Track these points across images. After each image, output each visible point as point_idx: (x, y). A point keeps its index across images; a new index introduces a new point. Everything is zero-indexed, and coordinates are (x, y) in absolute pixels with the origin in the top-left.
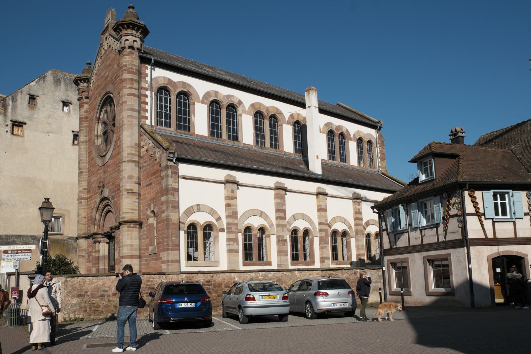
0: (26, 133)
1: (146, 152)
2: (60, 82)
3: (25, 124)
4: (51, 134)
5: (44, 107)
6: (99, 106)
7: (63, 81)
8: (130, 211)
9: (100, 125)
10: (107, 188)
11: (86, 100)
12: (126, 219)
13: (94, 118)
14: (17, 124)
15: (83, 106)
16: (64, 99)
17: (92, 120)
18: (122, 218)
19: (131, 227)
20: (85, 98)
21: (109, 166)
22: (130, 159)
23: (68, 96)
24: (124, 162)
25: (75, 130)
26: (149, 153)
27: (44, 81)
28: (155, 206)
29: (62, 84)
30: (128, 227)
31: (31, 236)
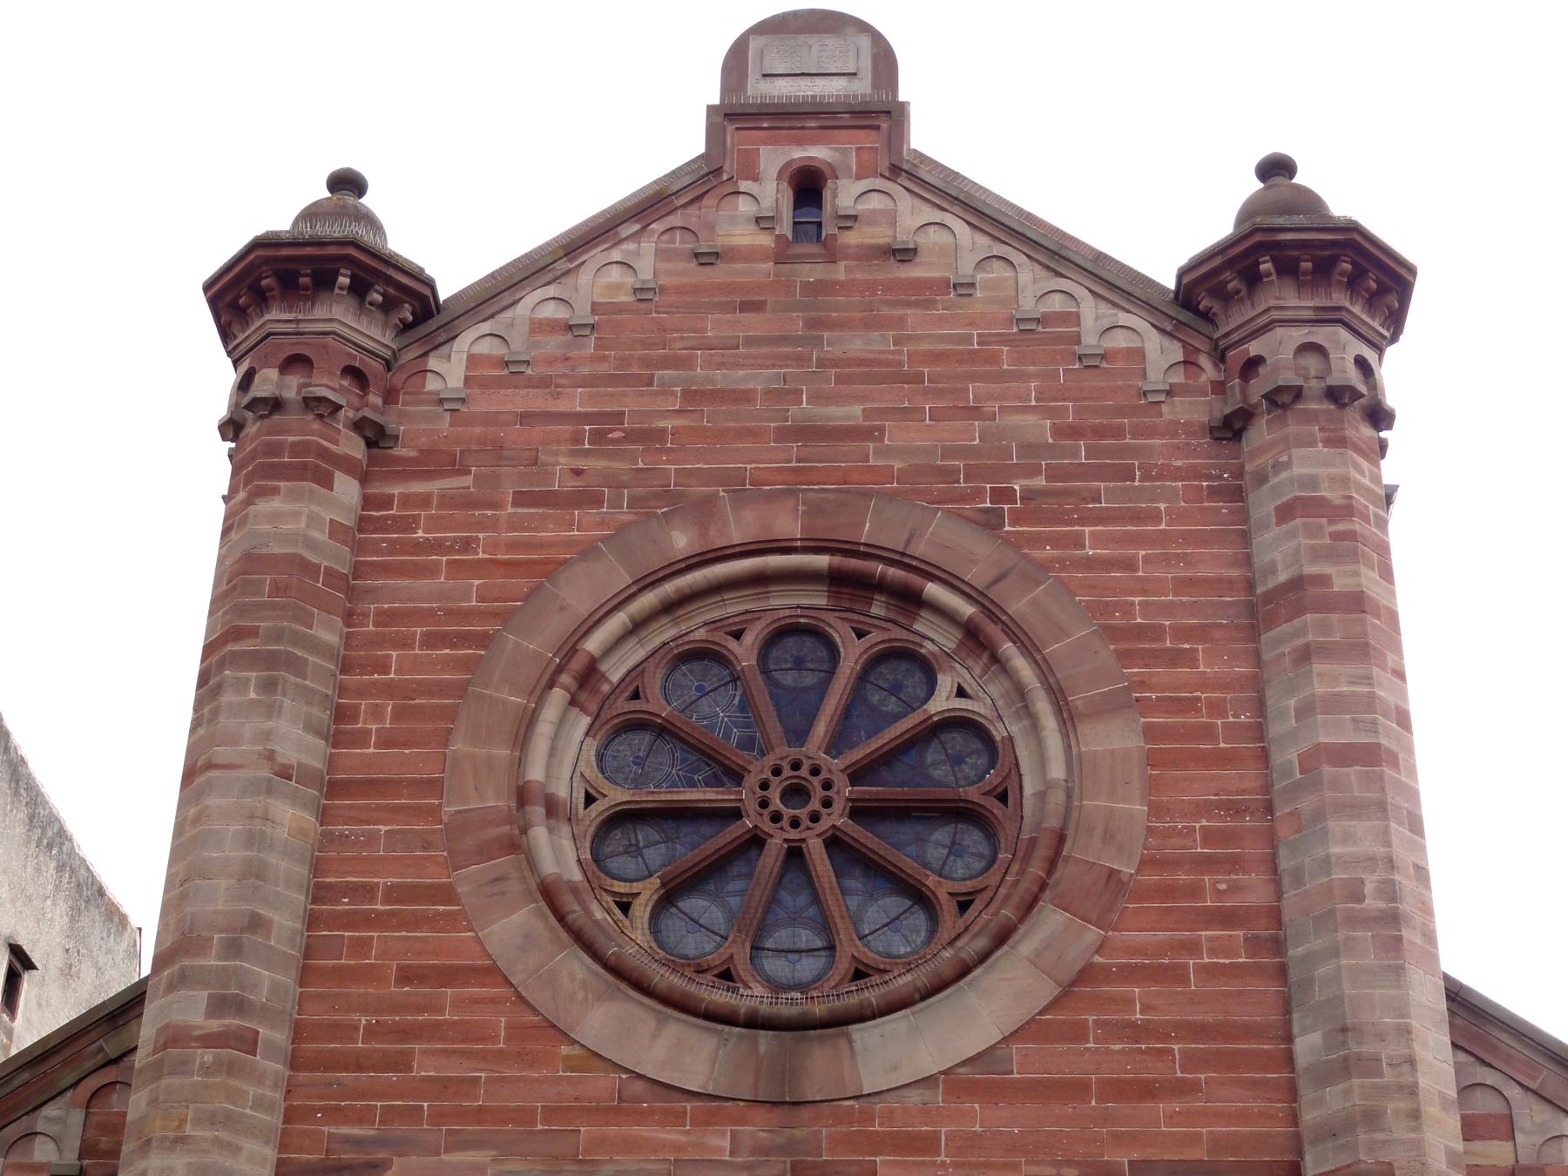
11: (353, 447)
13: (536, 642)
20: (359, 426)
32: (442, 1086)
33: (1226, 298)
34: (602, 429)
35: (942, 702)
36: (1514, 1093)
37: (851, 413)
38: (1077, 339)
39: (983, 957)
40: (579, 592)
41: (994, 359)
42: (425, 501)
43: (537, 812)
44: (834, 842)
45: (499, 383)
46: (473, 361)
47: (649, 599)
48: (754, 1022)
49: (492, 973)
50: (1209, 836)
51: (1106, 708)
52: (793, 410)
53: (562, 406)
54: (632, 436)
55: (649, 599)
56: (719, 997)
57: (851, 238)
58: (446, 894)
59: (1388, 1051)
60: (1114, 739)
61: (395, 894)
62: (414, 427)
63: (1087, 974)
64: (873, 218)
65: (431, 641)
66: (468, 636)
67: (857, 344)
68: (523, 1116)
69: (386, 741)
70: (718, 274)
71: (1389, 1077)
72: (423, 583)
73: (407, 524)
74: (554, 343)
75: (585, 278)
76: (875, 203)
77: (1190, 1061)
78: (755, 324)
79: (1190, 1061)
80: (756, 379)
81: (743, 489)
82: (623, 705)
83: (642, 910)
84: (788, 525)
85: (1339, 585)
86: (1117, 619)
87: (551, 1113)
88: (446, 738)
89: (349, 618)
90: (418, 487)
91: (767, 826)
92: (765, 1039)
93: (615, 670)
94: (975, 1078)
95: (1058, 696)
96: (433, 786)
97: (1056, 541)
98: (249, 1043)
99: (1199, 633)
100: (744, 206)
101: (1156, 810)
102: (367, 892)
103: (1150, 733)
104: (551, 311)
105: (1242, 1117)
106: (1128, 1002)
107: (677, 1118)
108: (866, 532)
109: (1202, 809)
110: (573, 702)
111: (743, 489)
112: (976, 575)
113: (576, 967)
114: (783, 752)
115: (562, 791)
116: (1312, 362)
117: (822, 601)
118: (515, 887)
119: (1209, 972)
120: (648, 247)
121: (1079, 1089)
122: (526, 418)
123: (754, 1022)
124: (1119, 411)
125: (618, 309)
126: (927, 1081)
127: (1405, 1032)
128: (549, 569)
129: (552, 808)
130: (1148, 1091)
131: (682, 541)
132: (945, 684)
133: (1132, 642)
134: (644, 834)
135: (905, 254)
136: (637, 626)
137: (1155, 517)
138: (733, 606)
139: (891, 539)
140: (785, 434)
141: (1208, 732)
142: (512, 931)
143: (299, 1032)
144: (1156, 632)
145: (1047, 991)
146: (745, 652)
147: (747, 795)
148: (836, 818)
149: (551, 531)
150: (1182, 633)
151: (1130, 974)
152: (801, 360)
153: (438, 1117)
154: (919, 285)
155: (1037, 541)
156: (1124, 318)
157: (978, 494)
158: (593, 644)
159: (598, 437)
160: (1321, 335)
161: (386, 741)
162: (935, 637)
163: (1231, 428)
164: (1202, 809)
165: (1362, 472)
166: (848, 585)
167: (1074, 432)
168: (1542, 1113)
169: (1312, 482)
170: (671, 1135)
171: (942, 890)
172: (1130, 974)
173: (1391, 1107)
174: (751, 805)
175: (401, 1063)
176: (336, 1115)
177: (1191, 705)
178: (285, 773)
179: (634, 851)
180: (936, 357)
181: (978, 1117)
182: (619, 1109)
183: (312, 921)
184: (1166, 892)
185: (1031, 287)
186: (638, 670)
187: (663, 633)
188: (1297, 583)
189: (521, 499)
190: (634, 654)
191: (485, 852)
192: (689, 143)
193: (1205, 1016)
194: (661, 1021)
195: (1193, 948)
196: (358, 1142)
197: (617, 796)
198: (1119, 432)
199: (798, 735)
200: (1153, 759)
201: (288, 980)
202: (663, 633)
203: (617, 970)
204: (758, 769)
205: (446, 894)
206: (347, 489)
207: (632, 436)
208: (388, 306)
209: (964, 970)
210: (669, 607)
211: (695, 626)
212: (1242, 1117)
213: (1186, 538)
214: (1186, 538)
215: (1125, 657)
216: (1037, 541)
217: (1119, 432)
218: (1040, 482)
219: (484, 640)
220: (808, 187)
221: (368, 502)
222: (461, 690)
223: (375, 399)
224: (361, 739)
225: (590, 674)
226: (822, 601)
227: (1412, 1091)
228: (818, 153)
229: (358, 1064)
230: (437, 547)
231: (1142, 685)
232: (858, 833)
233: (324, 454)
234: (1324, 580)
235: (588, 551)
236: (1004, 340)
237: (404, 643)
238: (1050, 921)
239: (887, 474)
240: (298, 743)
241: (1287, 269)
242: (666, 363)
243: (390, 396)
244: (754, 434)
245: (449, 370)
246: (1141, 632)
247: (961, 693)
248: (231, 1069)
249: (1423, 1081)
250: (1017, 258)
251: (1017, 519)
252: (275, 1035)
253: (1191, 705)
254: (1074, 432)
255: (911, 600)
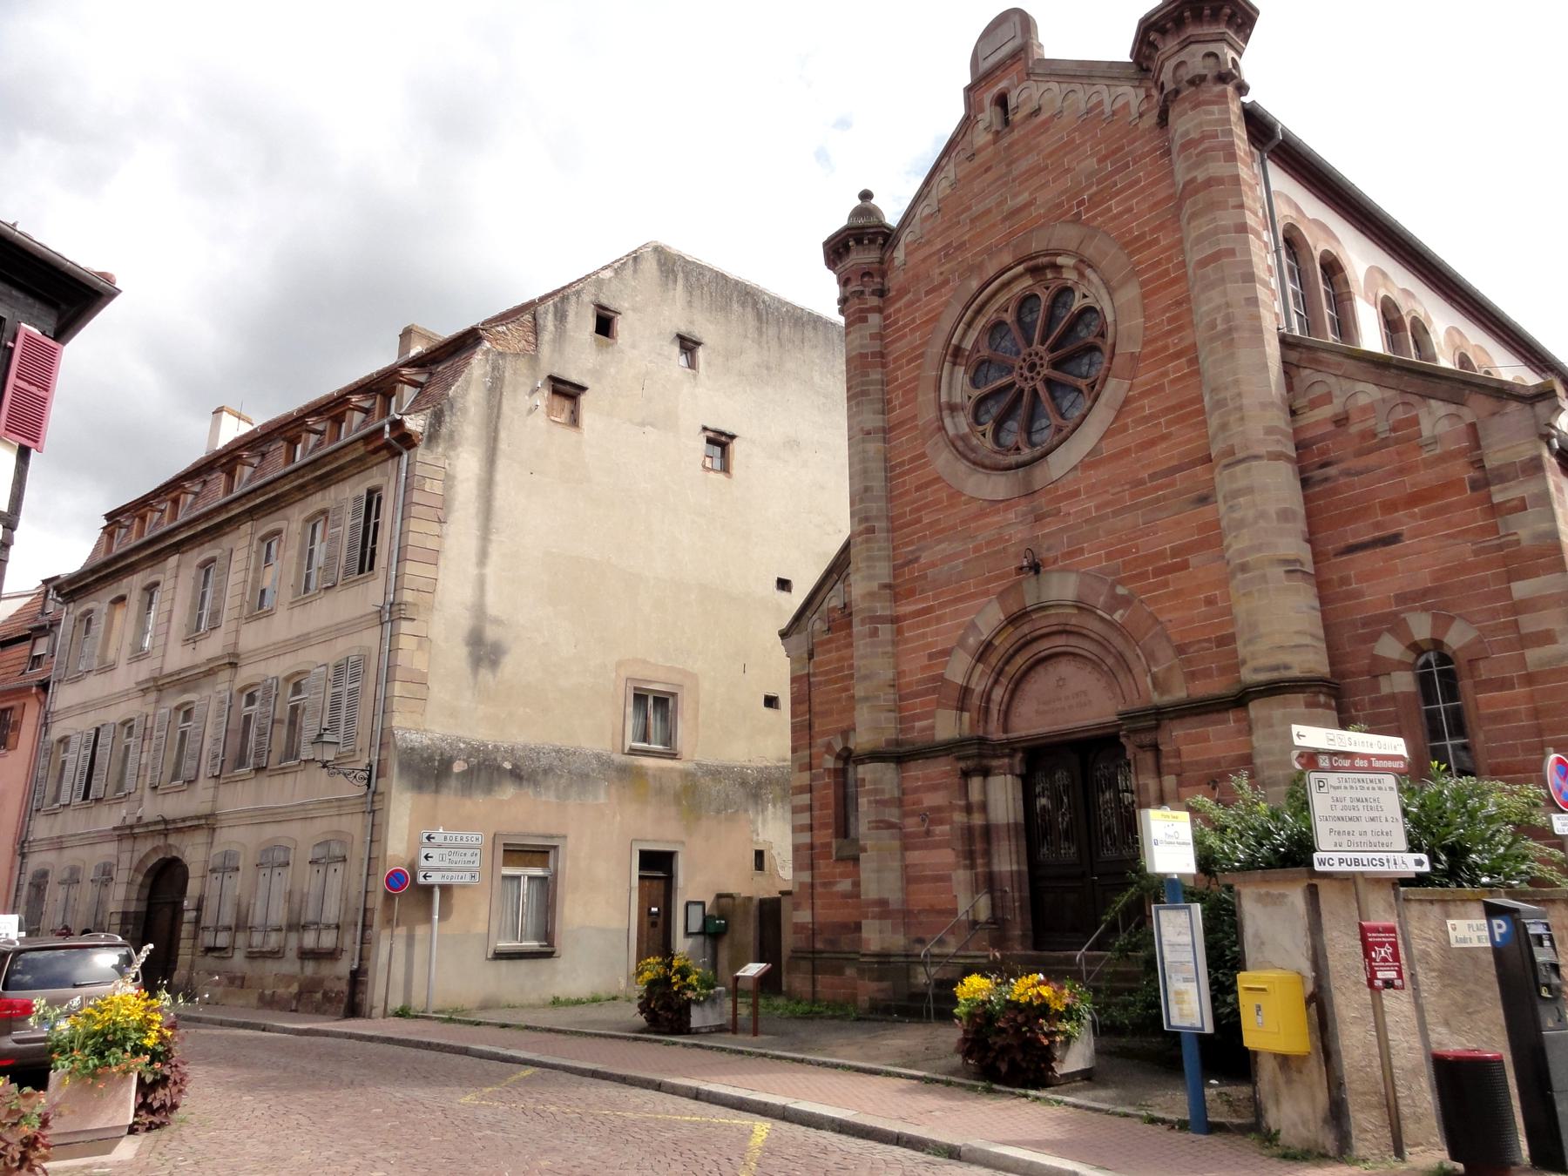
0: (586, 416)
1: (1331, 427)
2: (675, 281)
3: (583, 389)
4: (648, 429)
5: (634, 346)
6: (967, 308)
7: (680, 275)
8: (1308, 640)
9: (960, 370)
10: (1064, 569)
11: (874, 301)
12: (1295, 673)
13: (936, 349)
14: (566, 391)
15: (864, 320)
16: (683, 330)
17: (922, 355)
18: (1276, 668)
19: (1317, 705)
20: (873, 293)
21: (1076, 493)
22: (1279, 448)
23: (692, 322)
24: (1256, 457)
25: (709, 426)
26: (1354, 429)
27: (635, 271)
28: (1443, 621)
29: (680, 282)
30: (1309, 705)
31: (598, 757)
32: (931, 524)
33: (1150, 58)
34: (948, 252)
35: (1077, 304)
36: (1332, 380)
37: (1024, 197)
38: (1103, 112)
39: (1090, 409)
40: (946, 324)
41: (1073, 140)
42: (899, 310)
43: (946, 413)
44: (1049, 382)
45: (916, 250)
46: (907, 246)
47: (969, 313)
48: (1018, 466)
49: (938, 479)
50: (1170, 321)
51: (1124, 282)
52: (1005, 208)
53: (935, 248)
54: (957, 249)
55: (969, 313)
56: (1013, 459)
57: (1019, 116)
58: (923, 455)
59: (1228, 394)
60: (1130, 293)
61: (912, 460)
62: (895, 281)
63: (1127, 401)
64: (1025, 102)
65: (909, 362)
66: (917, 356)
67: (1023, 165)
68: (954, 527)
69: (901, 406)
70: (978, 160)
71: (1231, 405)
72: (904, 342)
73: (896, 322)
74: (928, 225)
75: (934, 192)
76: (1024, 95)
77: (1169, 424)
78: (990, 176)
79: (1169, 424)
80: (990, 202)
81: (990, 252)
82: (975, 356)
83: (989, 434)
84: (1007, 259)
85: (1200, 179)
86: (1128, 238)
87: (963, 522)
88: (916, 398)
89: (884, 366)
90: (897, 306)
91: (1023, 384)
92: (1021, 471)
93: (968, 345)
94: (1091, 461)
95: (1106, 283)
96: (914, 417)
97: (1101, 214)
98: (871, 530)
99: (1161, 227)
100: (981, 126)
101: (1147, 318)
102: (902, 464)
103: (1143, 284)
104: (927, 211)
105: (1189, 441)
106: (1143, 408)
107: (997, 512)
108: (1035, 247)
109: (1165, 310)
110: (954, 364)
111: (990, 252)
112: (1072, 246)
113: (962, 466)
114: (1024, 352)
115: (958, 400)
116: (1211, 61)
117: (1030, 282)
118: (941, 444)
119: (1173, 382)
120: (951, 165)
121: (1127, 451)
122: (924, 260)
123: (1018, 466)
124: (1121, 138)
125: (947, 197)
126: (1075, 468)
127: (1236, 382)
128: (935, 319)
129: (953, 408)
130: (1152, 443)
131: (975, 284)
132: (1077, 294)
133: (1132, 245)
134: (990, 403)
135: (1036, 112)
136: (969, 325)
137: (1137, 182)
138: (1002, 299)
139: (1042, 246)
140: (1005, 219)
141: (1167, 272)
142: (943, 461)
143: (891, 519)
144: (1143, 235)
145: (1113, 414)
146: (1009, 318)
147: (1015, 376)
148: (1045, 371)
149: (937, 301)
150: (1153, 231)
151: (1143, 395)
152: (1005, 184)
153: (932, 535)
154: (1045, 122)
155: (1094, 217)
156: (1120, 90)
157: (1071, 208)
158: (954, 341)
159: (946, 255)
160: (1182, 56)
161: (901, 406)
162: (1070, 276)
163: (1163, 120)
164: (1165, 310)
165: (1212, 113)
166: (1035, 271)
167: (1106, 158)
168: (1346, 384)
169: (1187, 133)
170: (996, 519)
171: (1082, 384)
172: (1143, 395)
173: (1232, 419)
174: (1017, 379)
175: (919, 520)
176: (906, 544)
177: (1159, 263)
178: (869, 433)
179: (988, 412)
180: (1051, 154)
181: (1095, 476)
182: (981, 514)
183: (888, 479)
184: (1154, 353)
185: (1082, 97)
186: (977, 341)
187: (981, 322)
188: (1186, 184)
189: (927, 293)
190: (973, 335)
191: (932, 436)
192: (960, 112)
193: (1173, 402)
194: (993, 478)
195: (1165, 374)
196: (912, 552)
197: (976, 393)
198: (1121, 148)
199: (1029, 343)
200: (1144, 296)
201: (883, 504)
202: (981, 322)
203: (974, 463)
204: (1018, 363)
205: (923, 455)
206: (874, 319)
207: (957, 249)
208: (872, 241)
209: (1084, 417)
210: (979, 311)
211: (990, 314)
212: (1189, 441)
213: (1153, 184)
214: (1153, 184)
215: (1131, 255)
216: (1094, 217)
217: (1121, 148)
218: (1094, 189)
219: (922, 355)
220: (1002, 101)
221: (886, 318)
222: (916, 378)
223: (877, 280)
224: (893, 410)
225: (958, 351)
226: (1030, 282)
227: (1240, 408)
228: (1002, 85)
229: (909, 525)
230: (905, 326)
231: (1139, 263)
232: (1056, 375)
233: (862, 310)
234: (1193, 180)
235: (947, 304)
236: (1075, 130)
237: (900, 368)
238: (1112, 383)
239: (1040, 216)
240: (873, 420)
241: (1163, 32)
242: (963, 212)
243: (883, 275)
244: (994, 225)
245: (900, 255)
246: (1137, 239)
247: (1085, 296)
248: (867, 541)
249: (1245, 401)
250: (1077, 87)
251: (1087, 211)
252: (881, 525)
253: (1159, 263)
254: (1106, 158)
255: (1057, 268)
